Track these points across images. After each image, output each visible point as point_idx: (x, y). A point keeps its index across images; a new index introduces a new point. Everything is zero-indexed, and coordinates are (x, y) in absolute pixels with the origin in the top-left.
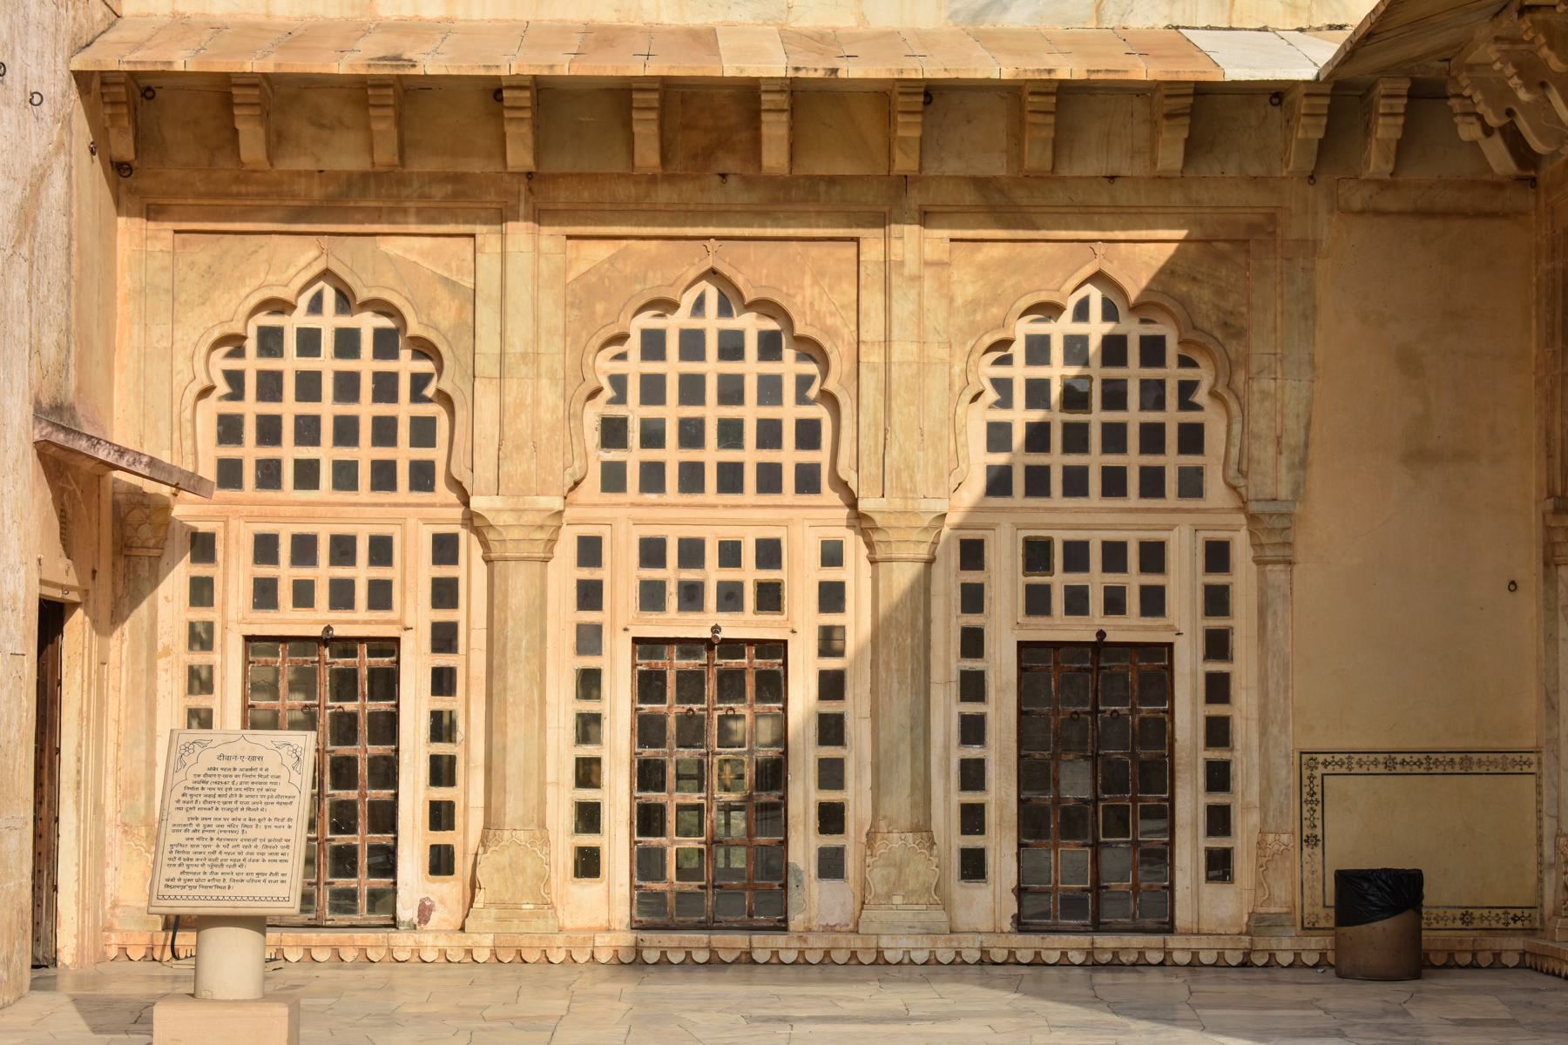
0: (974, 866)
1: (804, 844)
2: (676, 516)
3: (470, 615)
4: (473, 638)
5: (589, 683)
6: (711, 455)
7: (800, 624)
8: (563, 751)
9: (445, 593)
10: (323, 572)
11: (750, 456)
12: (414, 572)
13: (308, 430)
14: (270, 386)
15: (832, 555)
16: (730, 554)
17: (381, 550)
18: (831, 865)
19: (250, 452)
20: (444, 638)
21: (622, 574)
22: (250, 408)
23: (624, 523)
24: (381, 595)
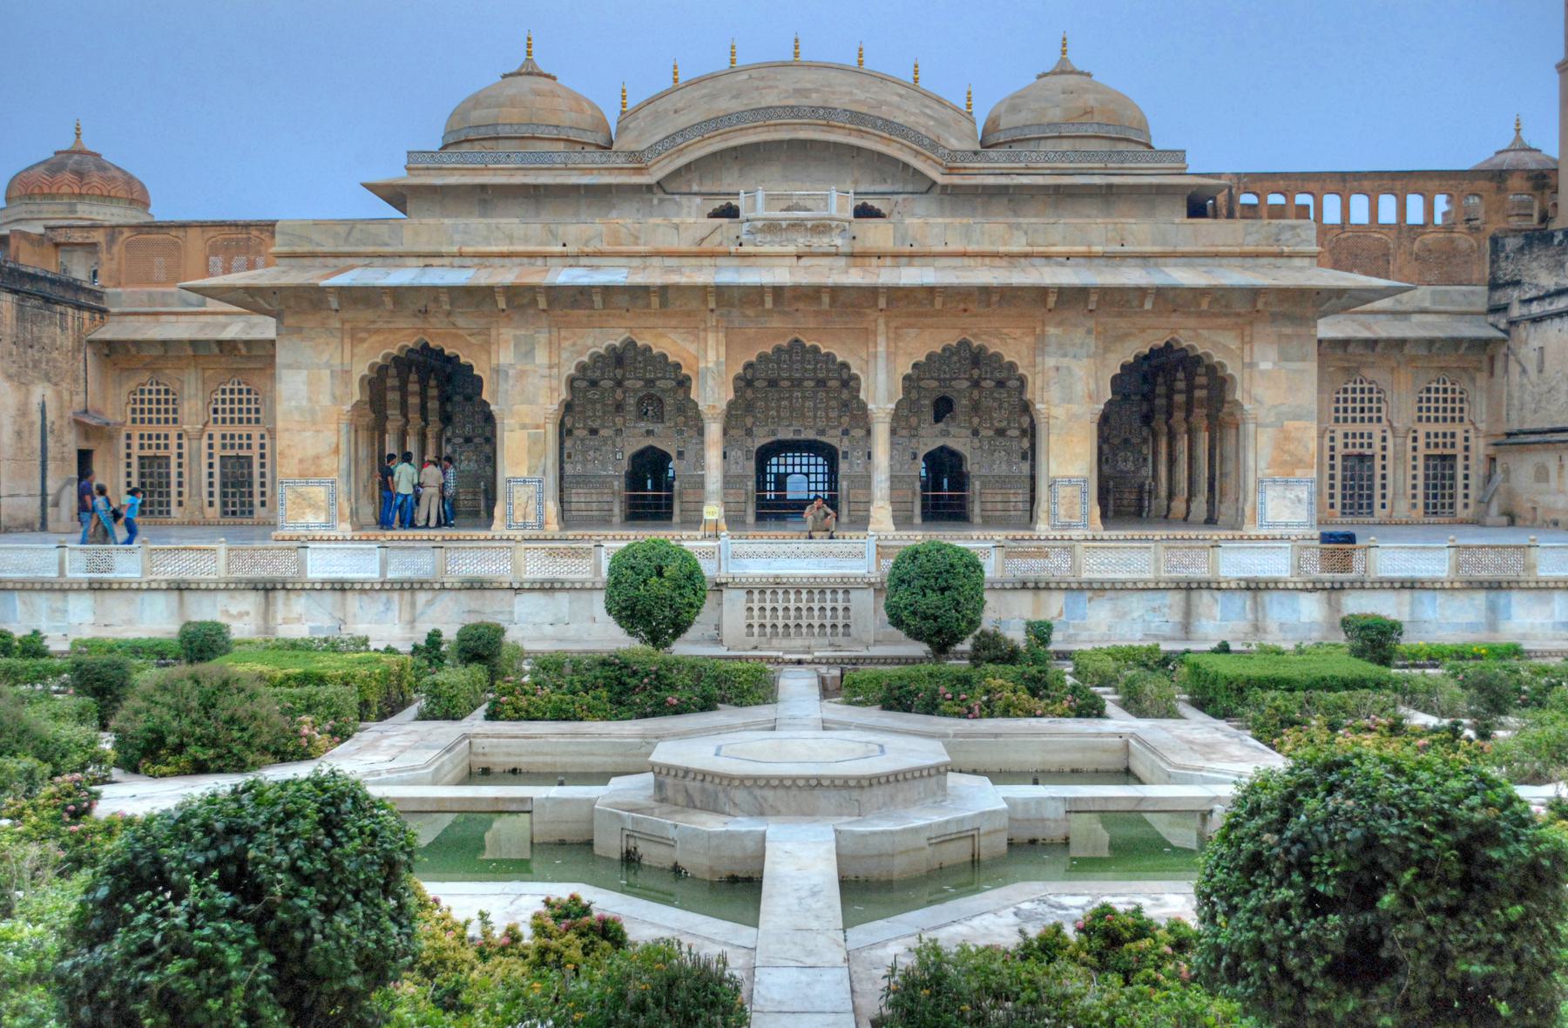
1: (257, 500)
2: (229, 429)
3: (185, 451)
4: (186, 455)
5: (211, 465)
6: (236, 415)
7: (255, 453)
8: (205, 480)
9: (180, 446)
10: (154, 442)
11: (245, 416)
12: (173, 442)
14: (142, 401)
15: (262, 437)
17: (166, 437)
18: (263, 504)
19: (138, 416)
20: (180, 456)
21: (217, 442)
22: (138, 406)
23: (217, 431)
24: (166, 446)
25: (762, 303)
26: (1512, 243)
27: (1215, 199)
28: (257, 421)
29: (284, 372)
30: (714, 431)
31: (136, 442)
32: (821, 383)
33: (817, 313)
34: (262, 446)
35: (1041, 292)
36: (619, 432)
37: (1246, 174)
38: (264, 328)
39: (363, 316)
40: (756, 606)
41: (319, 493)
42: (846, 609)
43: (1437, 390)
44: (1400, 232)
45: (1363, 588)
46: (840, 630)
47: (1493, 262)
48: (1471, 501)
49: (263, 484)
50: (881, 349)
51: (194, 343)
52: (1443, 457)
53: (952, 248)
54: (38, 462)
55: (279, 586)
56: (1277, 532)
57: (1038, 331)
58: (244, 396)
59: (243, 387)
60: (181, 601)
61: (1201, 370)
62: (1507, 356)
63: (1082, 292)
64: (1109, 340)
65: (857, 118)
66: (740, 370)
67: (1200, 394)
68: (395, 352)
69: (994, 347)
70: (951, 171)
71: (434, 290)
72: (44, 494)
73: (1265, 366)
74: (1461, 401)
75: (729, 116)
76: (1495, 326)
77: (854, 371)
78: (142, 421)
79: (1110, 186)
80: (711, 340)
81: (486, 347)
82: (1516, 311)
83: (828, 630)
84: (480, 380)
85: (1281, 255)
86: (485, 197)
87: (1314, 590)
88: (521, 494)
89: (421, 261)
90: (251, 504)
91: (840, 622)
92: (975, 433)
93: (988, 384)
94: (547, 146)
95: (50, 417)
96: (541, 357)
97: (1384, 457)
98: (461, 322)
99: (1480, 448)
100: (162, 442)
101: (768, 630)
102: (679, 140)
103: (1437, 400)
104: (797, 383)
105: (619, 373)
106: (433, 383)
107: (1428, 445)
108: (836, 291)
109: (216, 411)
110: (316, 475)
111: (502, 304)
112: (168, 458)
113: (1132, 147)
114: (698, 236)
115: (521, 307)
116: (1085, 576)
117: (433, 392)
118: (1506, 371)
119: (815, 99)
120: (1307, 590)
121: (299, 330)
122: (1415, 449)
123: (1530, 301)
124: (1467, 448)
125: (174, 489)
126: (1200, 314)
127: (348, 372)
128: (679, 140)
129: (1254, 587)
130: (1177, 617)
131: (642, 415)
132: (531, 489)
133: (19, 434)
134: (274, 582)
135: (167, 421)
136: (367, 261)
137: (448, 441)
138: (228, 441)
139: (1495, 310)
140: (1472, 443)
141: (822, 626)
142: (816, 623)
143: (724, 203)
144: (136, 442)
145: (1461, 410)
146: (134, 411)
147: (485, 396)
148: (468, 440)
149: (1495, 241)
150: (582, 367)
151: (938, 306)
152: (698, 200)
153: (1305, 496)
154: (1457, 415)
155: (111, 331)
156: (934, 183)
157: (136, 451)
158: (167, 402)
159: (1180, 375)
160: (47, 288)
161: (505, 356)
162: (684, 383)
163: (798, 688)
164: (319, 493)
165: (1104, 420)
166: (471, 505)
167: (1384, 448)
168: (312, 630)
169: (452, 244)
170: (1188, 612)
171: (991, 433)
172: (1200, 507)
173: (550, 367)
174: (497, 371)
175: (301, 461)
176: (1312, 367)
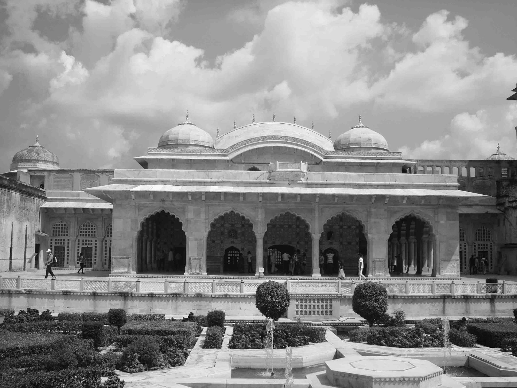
0: (105, 264)
1: (93, 262)
3: (70, 245)
6: (88, 234)
7: (93, 246)
9: (68, 243)
10: (60, 242)
11: (90, 234)
12: (66, 242)
13: (59, 231)
14: (57, 228)
15: (96, 241)
16: (89, 241)
17: (64, 240)
18: (95, 263)
20: (68, 247)
21: (81, 242)
23: (81, 239)
24: (64, 243)
25: (277, 199)
26: (504, 183)
27: (410, 168)
28: (95, 235)
30: (260, 243)
31: (54, 242)
32: (290, 226)
33: (295, 203)
34: (96, 244)
35: (370, 197)
36: (222, 242)
37: (420, 160)
38: (108, 206)
39: (143, 201)
40: (300, 304)
41: (126, 261)
42: (331, 306)
43: (481, 230)
44: (468, 179)
45: (502, 298)
46: (329, 313)
47: (497, 189)
48: (493, 266)
49: (95, 257)
50: (317, 215)
51: (75, 209)
52: (484, 252)
53: (340, 182)
54: (24, 248)
55: (130, 295)
56: (446, 277)
57: (368, 210)
58: (91, 227)
59: (90, 224)
60: (125, 303)
61: (413, 223)
62: (504, 220)
63: (383, 197)
64: (392, 213)
65: (296, 139)
66: (269, 222)
67: (412, 231)
68: (153, 213)
69: (354, 215)
70: (327, 157)
71: (167, 193)
72: (25, 259)
73: (442, 222)
74: (489, 234)
76: (500, 210)
77: (308, 222)
78: (56, 235)
79: (378, 163)
80: (260, 211)
81: (184, 212)
82: (507, 205)
83: (324, 313)
84: (181, 224)
85: (446, 186)
86: (174, 164)
87: (486, 299)
88: (194, 262)
89: (163, 183)
90: (91, 263)
91: (329, 310)
92: (341, 243)
93: (345, 227)
94: (194, 147)
95: (28, 233)
96: (203, 216)
97: (465, 252)
98: (175, 203)
99: (495, 249)
100: (62, 242)
101: (304, 313)
102: (238, 146)
103: (481, 233)
104: (282, 226)
105: (223, 222)
106: (155, 224)
107: (479, 248)
108: (302, 196)
109: (81, 232)
110: (125, 255)
111: (190, 198)
112: (64, 247)
113: (382, 151)
114: (256, 177)
115: (196, 200)
116: (410, 294)
117: (155, 227)
118: (504, 224)
119: (282, 134)
120: (484, 299)
122: (475, 249)
123: (513, 202)
124: (491, 249)
125: (66, 258)
126: (421, 205)
127: (136, 220)
128: (238, 146)
129: (466, 298)
130: (441, 308)
131: (230, 236)
132: (199, 260)
133: (19, 238)
134: (128, 294)
135: (64, 235)
137: (159, 243)
138: (84, 242)
139: (500, 204)
140: (493, 247)
141: (322, 312)
142: (320, 310)
144: (54, 242)
145: (489, 237)
146: (54, 231)
147: (183, 229)
148: (165, 243)
149: (499, 183)
150: (215, 220)
151: (336, 201)
152: (244, 165)
153: (456, 265)
154: (488, 238)
155: (47, 204)
156: (321, 161)
157: (54, 245)
158: (65, 228)
159: (404, 224)
160: (30, 190)
161: (190, 215)
162: (251, 226)
163: (330, 335)
164: (126, 261)
165: (390, 240)
166: (176, 265)
167: (465, 249)
168: (141, 311)
169: (173, 177)
170: (444, 307)
171: (346, 244)
172: (413, 270)
173: (206, 219)
174: (187, 220)
175: (119, 250)
176: (457, 223)
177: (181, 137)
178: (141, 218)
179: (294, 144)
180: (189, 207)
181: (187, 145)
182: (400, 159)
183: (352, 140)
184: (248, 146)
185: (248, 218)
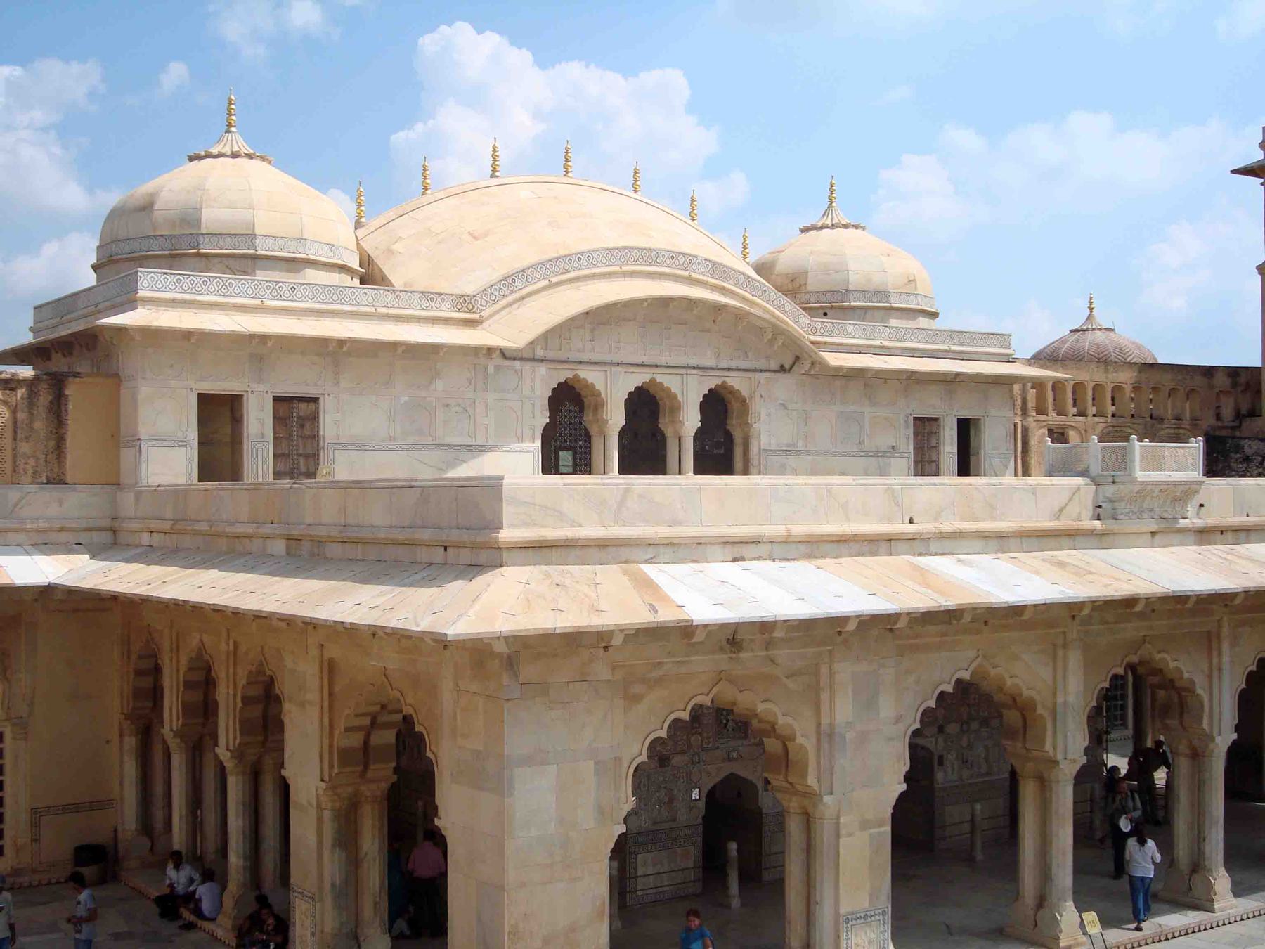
29: (518, 771)
75: (579, 256)
81: (814, 692)
89: (730, 551)
96: (887, 707)
102: (519, 284)
121: (543, 686)
127: (618, 760)
136: (650, 553)
143: (570, 375)
152: (542, 370)
161: (843, 710)
177: (212, 217)
178: (635, 749)
179: (714, 288)
180: (837, 666)
181: (295, 264)
182: (1009, 359)
183: (855, 280)
184: (557, 284)
185: (1033, 694)
